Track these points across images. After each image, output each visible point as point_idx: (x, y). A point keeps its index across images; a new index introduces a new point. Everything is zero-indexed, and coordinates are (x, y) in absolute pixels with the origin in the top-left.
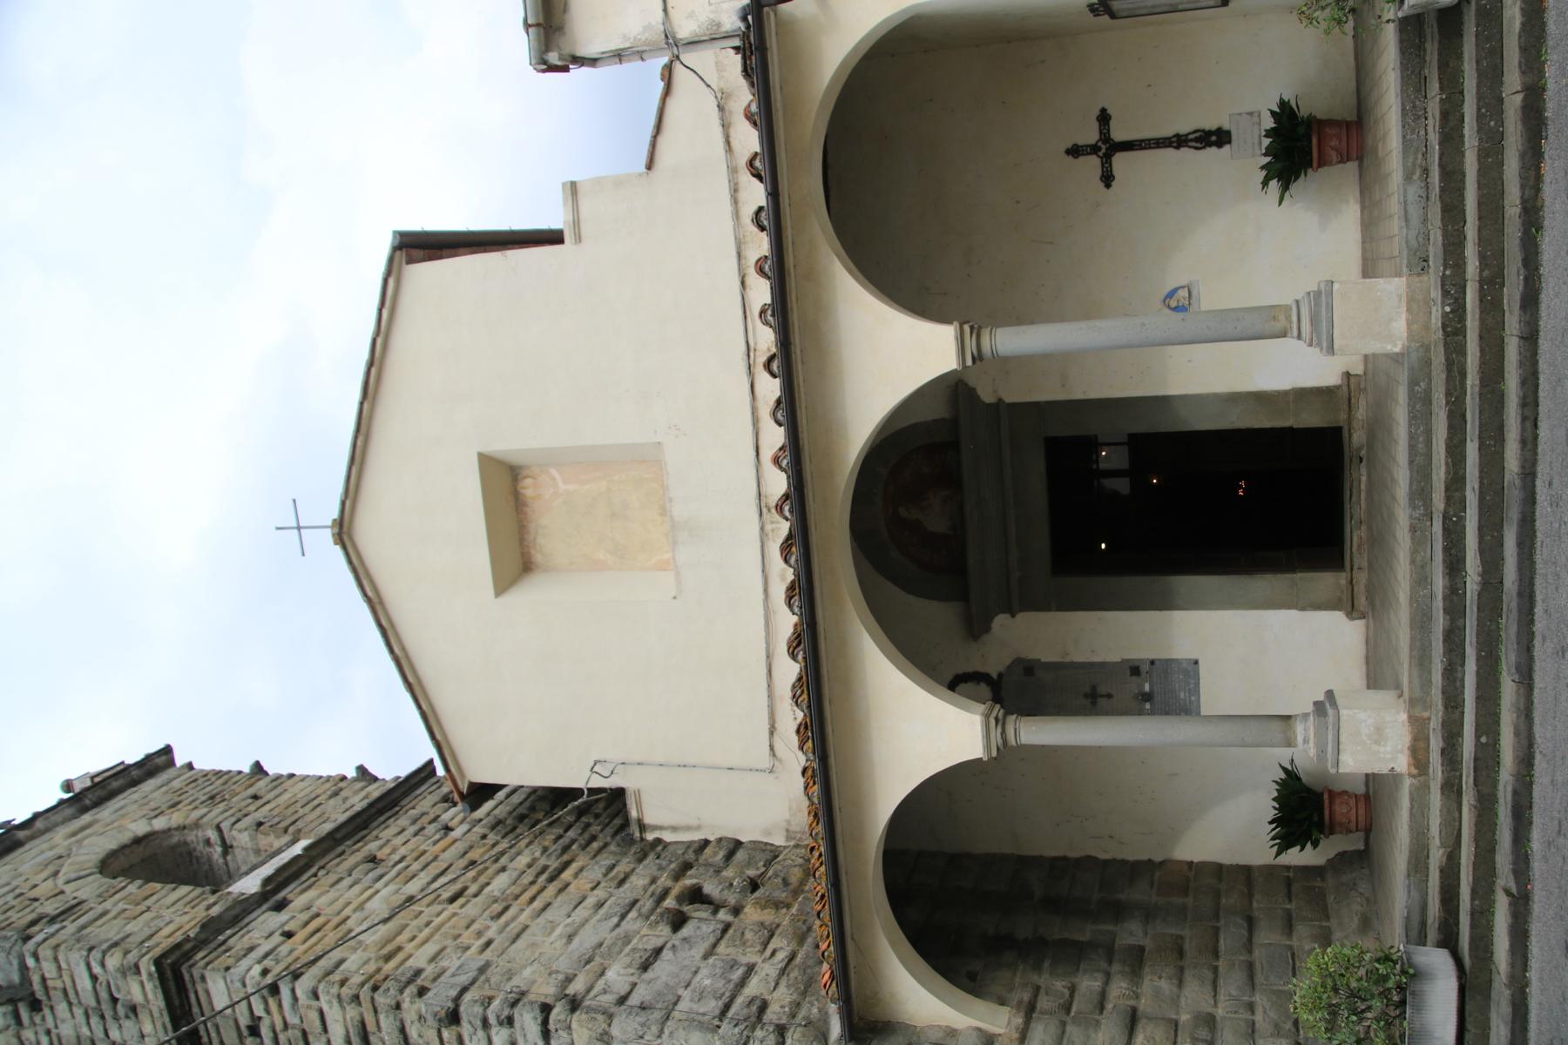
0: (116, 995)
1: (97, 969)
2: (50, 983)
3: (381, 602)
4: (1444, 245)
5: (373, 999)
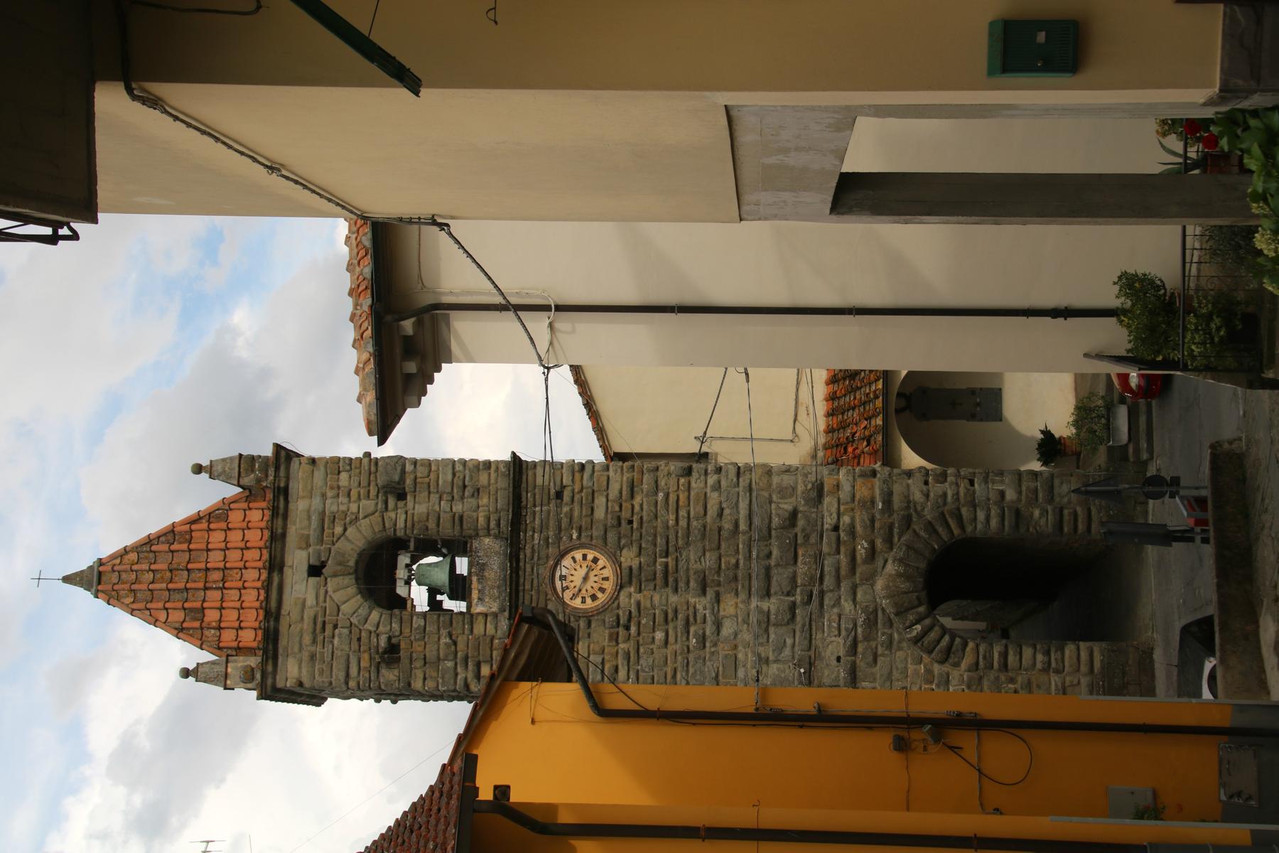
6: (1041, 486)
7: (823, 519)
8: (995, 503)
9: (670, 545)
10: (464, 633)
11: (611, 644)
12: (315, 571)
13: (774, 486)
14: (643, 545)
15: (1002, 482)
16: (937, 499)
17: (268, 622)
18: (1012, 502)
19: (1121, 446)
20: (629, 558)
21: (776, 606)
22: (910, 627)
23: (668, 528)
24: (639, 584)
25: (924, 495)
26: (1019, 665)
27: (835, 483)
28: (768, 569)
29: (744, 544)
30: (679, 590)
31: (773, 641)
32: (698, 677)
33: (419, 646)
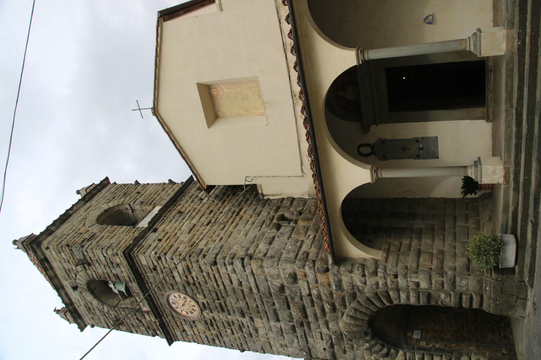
0: (112, 261)
1: (105, 255)
2: (92, 259)
3: (171, 132)
4: (519, 22)
5: (190, 259)
15: (417, 277)
17: (68, 307)
20: (200, 297)
23: (215, 288)
27: (303, 275)
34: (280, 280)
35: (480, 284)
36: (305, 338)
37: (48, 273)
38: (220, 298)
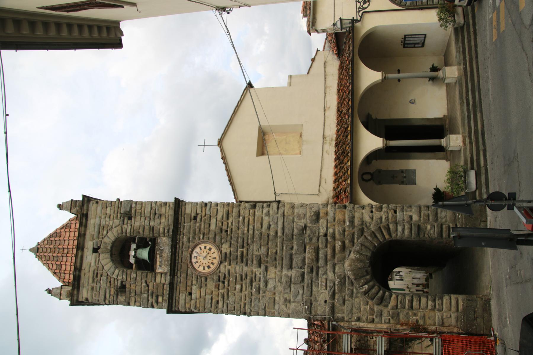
2: (137, 211)
6: (431, 213)
7: (319, 230)
8: (407, 222)
9: (245, 242)
10: (152, 281)
11: (215, 290)
12: (95, 250)
13: (295, 214)
14: (232, 242)
15: (411, 211)
16: (377, 220)
18: (416, 221)
19: (472, 192)
20: (225, 248)
21: (295, 274)
22: (362, 286)
23: (244, 234)
24: (229, 261)
25: (370, 218)
26: (419, 307)
27: (325, 212)
28: (291, 255)
29: (280, 242)
30: (248, 265)
31: (293, 292)
32: (256, 308)
33: (133, 286)
34: (305, 220)
35: (454, 214)
36: (310, 287)
37: (81, 228)
38: (245, 245)
